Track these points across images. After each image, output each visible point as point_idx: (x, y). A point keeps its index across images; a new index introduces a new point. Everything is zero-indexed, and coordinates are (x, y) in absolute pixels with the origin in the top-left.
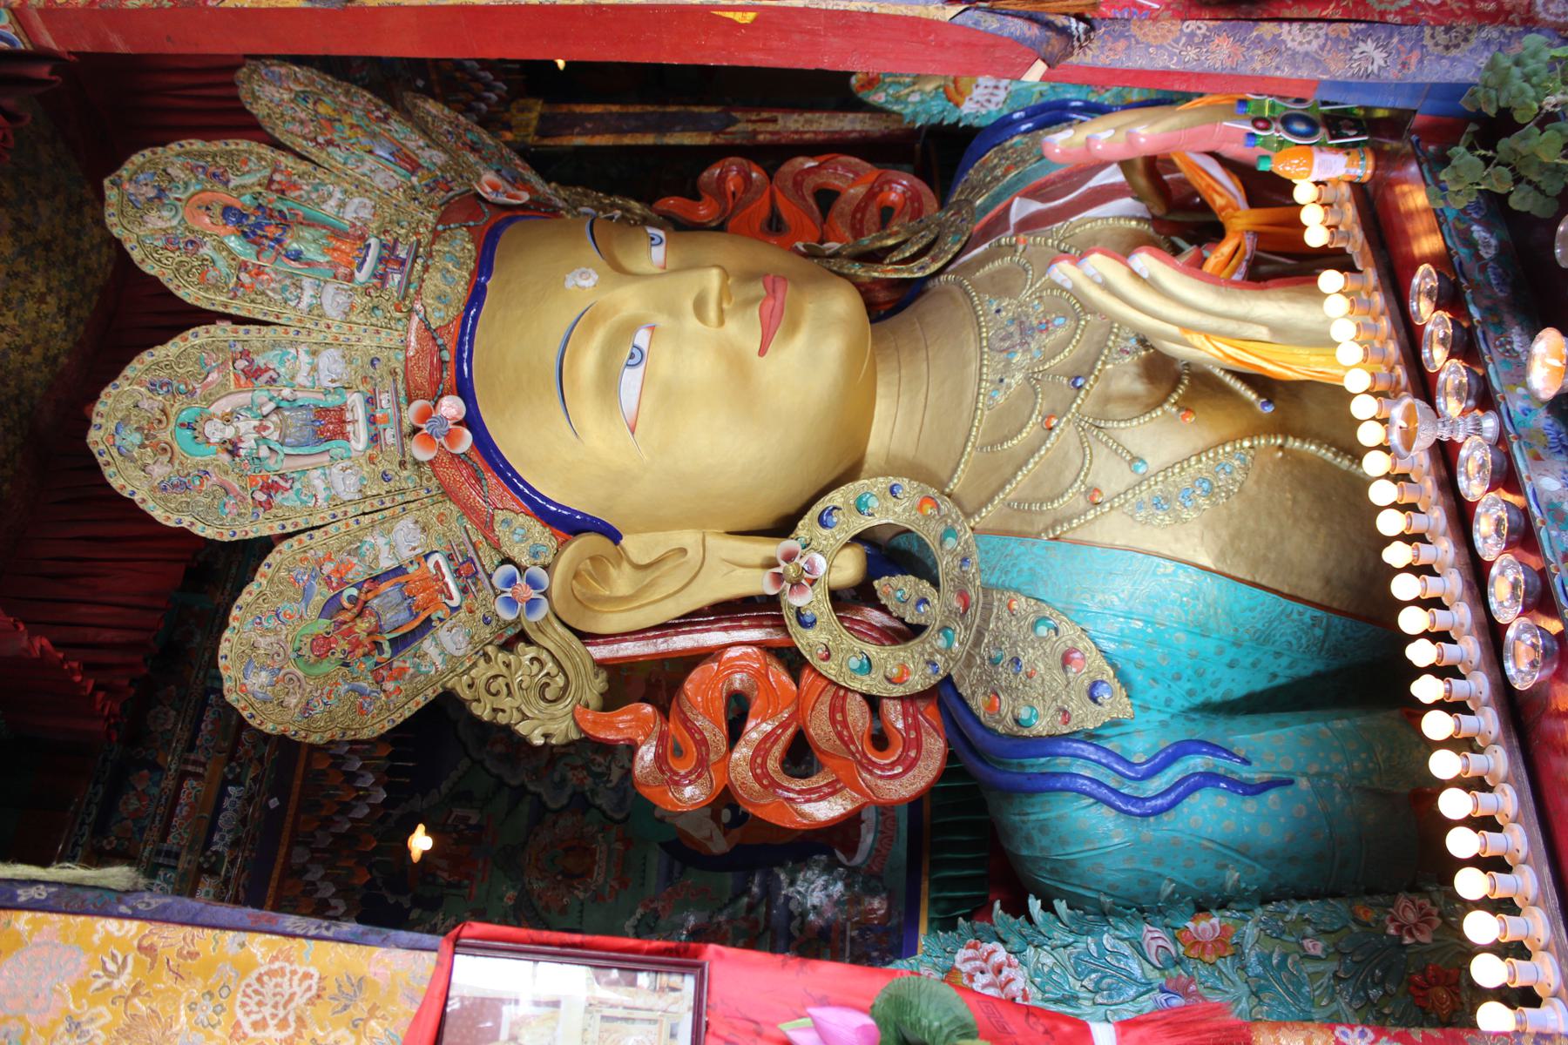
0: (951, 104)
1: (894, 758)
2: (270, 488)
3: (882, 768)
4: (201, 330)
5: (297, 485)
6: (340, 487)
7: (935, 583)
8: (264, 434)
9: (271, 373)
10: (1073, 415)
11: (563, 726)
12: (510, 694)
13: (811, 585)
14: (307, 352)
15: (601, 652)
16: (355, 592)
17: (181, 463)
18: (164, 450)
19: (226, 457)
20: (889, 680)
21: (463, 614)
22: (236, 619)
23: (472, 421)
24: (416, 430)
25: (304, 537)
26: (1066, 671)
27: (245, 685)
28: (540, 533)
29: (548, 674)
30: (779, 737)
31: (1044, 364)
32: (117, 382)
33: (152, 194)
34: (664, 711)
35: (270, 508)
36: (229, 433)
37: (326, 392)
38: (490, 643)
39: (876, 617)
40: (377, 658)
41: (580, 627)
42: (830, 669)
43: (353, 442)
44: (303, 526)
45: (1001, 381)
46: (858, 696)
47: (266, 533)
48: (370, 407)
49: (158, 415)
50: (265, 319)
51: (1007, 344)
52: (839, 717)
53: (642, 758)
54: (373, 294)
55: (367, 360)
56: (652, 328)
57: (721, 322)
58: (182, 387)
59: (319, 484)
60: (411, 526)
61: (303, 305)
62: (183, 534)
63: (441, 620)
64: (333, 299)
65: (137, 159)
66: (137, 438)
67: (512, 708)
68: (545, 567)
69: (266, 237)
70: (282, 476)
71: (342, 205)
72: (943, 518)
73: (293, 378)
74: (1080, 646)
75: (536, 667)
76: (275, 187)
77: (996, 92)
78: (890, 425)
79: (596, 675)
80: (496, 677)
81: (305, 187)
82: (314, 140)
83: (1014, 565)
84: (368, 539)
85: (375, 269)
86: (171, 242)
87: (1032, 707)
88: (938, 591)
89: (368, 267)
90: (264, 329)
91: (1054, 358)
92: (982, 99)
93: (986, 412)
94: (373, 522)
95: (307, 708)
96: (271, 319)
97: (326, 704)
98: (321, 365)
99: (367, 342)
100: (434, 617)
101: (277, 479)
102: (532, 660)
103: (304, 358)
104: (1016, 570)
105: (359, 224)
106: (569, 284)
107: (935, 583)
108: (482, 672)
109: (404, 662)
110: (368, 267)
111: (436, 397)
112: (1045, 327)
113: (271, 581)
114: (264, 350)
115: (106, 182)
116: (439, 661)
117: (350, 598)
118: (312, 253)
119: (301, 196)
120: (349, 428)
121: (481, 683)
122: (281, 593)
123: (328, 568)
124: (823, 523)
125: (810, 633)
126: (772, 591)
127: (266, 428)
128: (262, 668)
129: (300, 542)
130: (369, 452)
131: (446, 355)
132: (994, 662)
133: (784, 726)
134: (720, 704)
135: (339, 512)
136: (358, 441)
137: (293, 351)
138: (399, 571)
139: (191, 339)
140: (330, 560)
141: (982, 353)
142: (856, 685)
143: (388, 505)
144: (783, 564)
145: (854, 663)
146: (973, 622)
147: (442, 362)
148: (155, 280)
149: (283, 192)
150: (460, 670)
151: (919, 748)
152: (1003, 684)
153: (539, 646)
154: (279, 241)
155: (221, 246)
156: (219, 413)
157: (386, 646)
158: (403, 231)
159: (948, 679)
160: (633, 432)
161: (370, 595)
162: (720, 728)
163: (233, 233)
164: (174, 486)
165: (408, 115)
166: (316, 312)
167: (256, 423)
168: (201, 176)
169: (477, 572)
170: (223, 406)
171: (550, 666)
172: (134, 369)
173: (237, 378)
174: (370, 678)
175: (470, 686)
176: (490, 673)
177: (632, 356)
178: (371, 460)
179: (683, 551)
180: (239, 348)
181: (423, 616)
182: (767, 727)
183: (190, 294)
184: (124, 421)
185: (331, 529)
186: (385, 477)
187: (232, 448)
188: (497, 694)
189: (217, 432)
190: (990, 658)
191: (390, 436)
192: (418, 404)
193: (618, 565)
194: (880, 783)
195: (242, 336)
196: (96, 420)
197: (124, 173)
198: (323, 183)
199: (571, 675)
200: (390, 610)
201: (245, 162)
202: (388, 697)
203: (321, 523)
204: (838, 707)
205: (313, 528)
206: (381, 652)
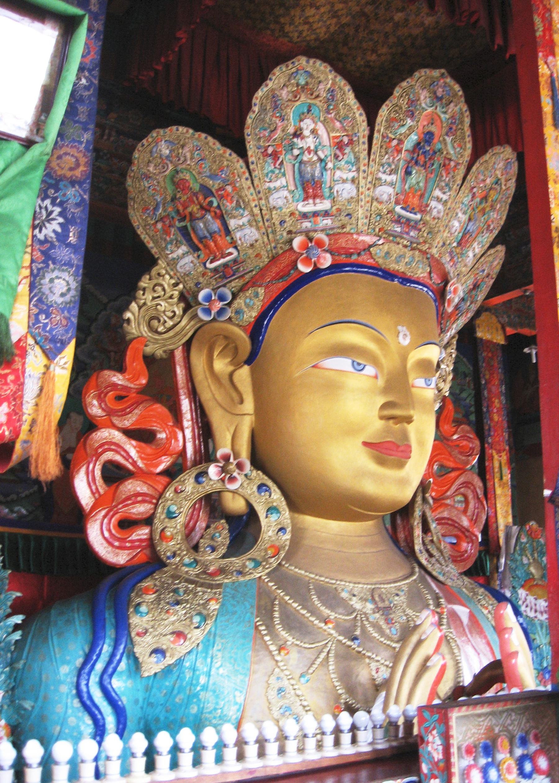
0: (523, 583)
1: (113, 531)
2: (275, 156)
4: (364, 117)
5: (277, 171)
6: (276, 195)
7: (224, 557)
8: (306, 152)
9: (341, 157)
11: (134, 331)
12: (154, 298)
13: (221, 479)
14: (354, 177)
15: (179, 355)
16: (215, 204)
17: (288, 106)
18: (296, 97)
19: (291, 130)
20: (163, 530)
21: (201, 269)
22: (199, 136)
23: (317, 273)
24: (311, 240)
25: (247, 175)
26: (173, 633)
27: (161, 141)
28: (250, 315)
29: (165, 322)
30: (127, 460)
33: (439, 94)
34: (142, 391)
35: (264, 156)
36: (306, 133)
37: (331, 188)
38: (184, 287)
39: (202, 524)
40: (177, 218)
41: (194, 342)
42: (169, 494)
43: (302, 203)
44: (253, 175)
45: (354, 595)
46: (152, 512)
47: (250, 153)
48: (323, 213)
49: (315, 94)
50: (372, 153)
52: (140, 499)
53: (114, 376)
54: (389, 215)
55: (351, 212)
56: (376, 377)
57: (381, 418)
58: (332, 107)
59: (278, 184)
60: (254, 238)
62: (249, 107)
63: (199, 256)
65: (457, 87)
66: (302, 82)
67: (145, 299)
68: (230, 318)
69: (418, 155)
70: (282, 163)
71: (438, 200)
72: (266, 560)
73: (338, 168)
74: (187, 643)
75: (171, 314)
76: (447, 162)
77: (533, 610)
79: (165, 352)
80: (164, 290)
83: (238, 602)
84: (246, 213)
85: (403, 217)
86: (411, 102)
87: (147, 613)
88: (220, 558)
89: (403, 213)
90: (366, 152)
92: (528, 602)
95: (147, 177)
96: (372, 157)
97: (149, 187)
99: (361, 211)
101: (280, 160)
102: (174, 312)
103: (351, 175)
104: (235, 603)
105: (429, 209)
106: (400, 328)
107: (224, 557)
108: (167, 281)
109: (174, 235)
110: (403, 213)
111: (330, 251)
112: (388, 621)
113: (221, 156)
114: (355, 153)
115: (443, 71)
116: (174, 255)
117: (211, 202)
120: (311, 201)
121: (160, 281)
122: (215, 162)
123: (229, 189)
124: (260, 487)
125: (192, 480)
126: (219, 454)
127: (309, 153)
129: (244, 173)
130: (297, 213)
131: (354, 257)
132: (176, 591)
133: (134, 463)
135: (261, 195)
136: (303, 206)
137: (354, 169)
138: (228, 232)
139: (359, 112)
140: (233, 191)
141: (372, 584)
142: (160, 510)
143: (266, 224)
144: (235, 462)
145: (174, 508)
146: (201, 578)
147: (351, 254)
148: (391, 94)
149: (444, 165)
150: (168, 269)
151: (120, 548)
152: (162, 596)
153: (182, 317)
154: (416, 163)
156: (317, 127)
157: (183, 224)
158: (425, 235)
159: (165, 565)
160: (313, 367)
161: (213, 214)
162: (132, 425)
163: (419, 137)
164: (275, 102)
165: (492, 245)
166: (376, 182)
168: (450, 121)
169: (227, 278)
171: (170, 323)
174: (164, 214)
175: (159, 274)
176: (166, 286)
177: (359, 364)
178: (292, 214)
179: (242, 401)
180: (355, 139)
181: (200, 246)
182: (133, 453)
183: (384, 112)
184: (310, 75)
185: (252, 190)
186: (282, 222)
187: (298, 134)
188: (155, 291)
189: (307, 125)
190: (178, 588)
191: (306, 225)
192: (326, 239)
193: (231, 363)
194: (98, 522)
195: (362, 140)
196: (312, 61)
197: (449, 80)
198: (450, 189)
201: (459, 146)
202: (153, 224)
203: (255, 185)
204: (144, 498)
206: (180, 221)
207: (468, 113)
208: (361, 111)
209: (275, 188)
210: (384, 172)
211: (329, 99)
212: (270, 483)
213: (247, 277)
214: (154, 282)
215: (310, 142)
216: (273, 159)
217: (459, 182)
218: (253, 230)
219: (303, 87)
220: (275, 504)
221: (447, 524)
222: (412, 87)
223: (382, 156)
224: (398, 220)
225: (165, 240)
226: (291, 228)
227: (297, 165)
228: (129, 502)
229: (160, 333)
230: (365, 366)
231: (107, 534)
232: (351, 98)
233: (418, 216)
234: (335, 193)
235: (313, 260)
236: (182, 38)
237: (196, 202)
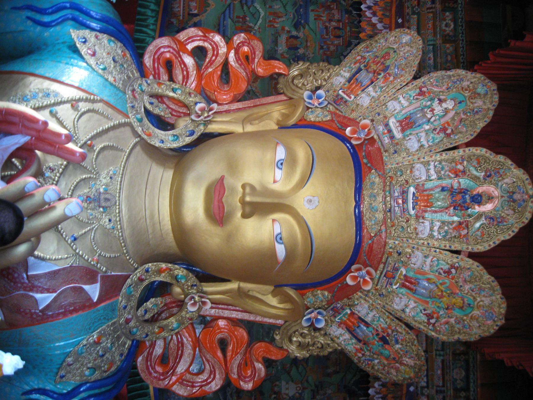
3: (169, 52)
5: (412, 98)
8: (430, 109)
9: (436, 132)
10: (80, 143)
18: (466, 90)
19: (442, 97)
21: (338, 89)
25: (404, 84)
28: (312, 117)
31: (90, 177)
32: (494, 107)
36: (444, 105)
37: (410, 134)
43: (395, 121)
47: (418, 80)
51: (107, 196)
52: (185, 73)
53: (260, 52)
58: (469, 114)
59: (403, 101)
61: (432, 164)
63: (345, 84)
64: (420, 171)
70: (417, 99)
73: (427, 134)
78: (163, 179)
81: (451, 231)
82: (456, 269)
84: (379, 93)
89: (410, 196)
91: (85, 178)
93: (119, 166)
94: (379, 99)
98: (416, 142)
100: (347, 83)
102: (307, 84)
103: (425, 143)
105: (421, 221)
110: (410, 196)
114: (442, 140)
118: (437, 193)
119: (452, 224)
120: (398, 124)
123: (391, 78)
127: (430, 111)
128: (406, 43)
133: (207, 68)
134: (233, 79)
137: (430, 144)
140: (391, 81)
145: (179, 92)
148: (497, 153)
155: (475, 179)
162: (231, 66)
167: (435, 112)
170: (451, 114)
171: (300, 85)
172: (491, 113)
173: (449, 125)
177: (282, 164)
178: (385, 117)
185: (394, 90)
187: (441, 101)
188: (318, 71)
189: (450, 105)
196: (495, 92)
199: (291, 85)
200: (364, 77)
205: (401, 88)
207: (512, 234)
208: (475, 134)
209: (400, 102)
210: (435, 167)
211: (473, 111)
212: (195, 137)
213: (338, 112)
214: (324, 69)
215: (438, 109)
216: (419, 93)
217: (453, 248)
218: (369, 101)
219: (475, 93)
220: (181, 139)
221: (178, 350)
222: (510, 169)
223: (446, 161)
224: (404, 193)
225: (351, 64)
226: (376, 120)
227: (420, 108)
228: (183, 66)
229: (293, 81)
230: (281, 169)
231: (162, 50)
232: (481, 125)
233: (412, 212)
234: (409, 138)
235: (355, 136)
236: (489, 60)
237: (378, 66)
